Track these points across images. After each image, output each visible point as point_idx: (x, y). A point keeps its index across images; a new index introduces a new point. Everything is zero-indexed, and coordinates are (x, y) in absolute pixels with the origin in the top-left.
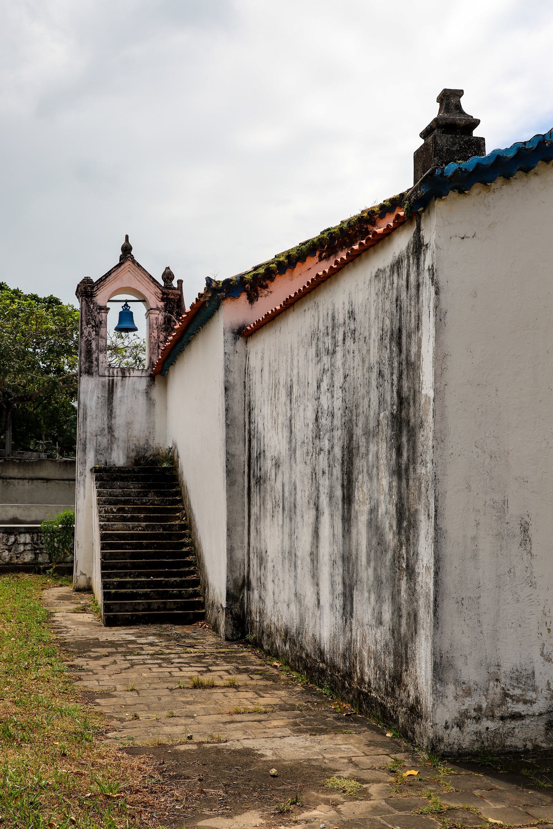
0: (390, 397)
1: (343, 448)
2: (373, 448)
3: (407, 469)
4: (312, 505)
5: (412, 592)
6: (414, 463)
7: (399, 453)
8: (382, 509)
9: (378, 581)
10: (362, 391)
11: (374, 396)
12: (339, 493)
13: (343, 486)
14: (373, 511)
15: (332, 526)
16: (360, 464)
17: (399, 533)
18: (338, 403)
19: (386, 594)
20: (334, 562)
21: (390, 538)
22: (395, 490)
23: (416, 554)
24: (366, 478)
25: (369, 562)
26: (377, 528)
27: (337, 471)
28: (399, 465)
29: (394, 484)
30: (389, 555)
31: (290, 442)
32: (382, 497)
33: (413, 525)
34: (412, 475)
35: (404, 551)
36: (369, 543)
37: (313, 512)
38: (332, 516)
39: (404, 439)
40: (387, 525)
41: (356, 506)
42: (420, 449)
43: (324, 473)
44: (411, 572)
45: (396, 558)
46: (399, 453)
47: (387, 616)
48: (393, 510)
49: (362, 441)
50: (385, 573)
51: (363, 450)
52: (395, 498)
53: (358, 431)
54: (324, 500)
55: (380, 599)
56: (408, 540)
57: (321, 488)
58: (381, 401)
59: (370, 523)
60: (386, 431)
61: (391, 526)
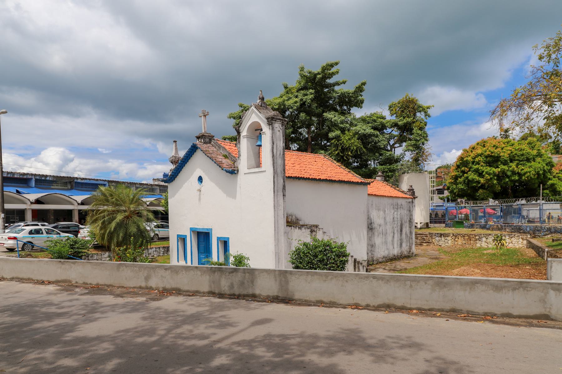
0: (409, 218)
2: (406, 224)
5: (412, 241)
7: (410, 225)
9: (407, 241)
10: (404, 216)
11: (406, 217)
12: (399, 230)
14: (406, 232)
15: (398, 235)
18: (399, 217)
19: (408, 242)
20: (398, 241)
21: (409, 235)
27: (399, 227)
31: (385, 221)
33: (412, 233)
36: (405, 237)
37: (393, 234)
38: (398, 234)
41: (403, 232)
44: (412, 238)
45: (410, 237)
46: (410, 225)
47: (408, 244)
48: (409, 232)
49: (404, 223)
50: (408, 240)
53: (403, 222)
54: (396, 232)
55: (407, 243)
58: (407, 218)
59: (405, 234)
60: (408, 222)
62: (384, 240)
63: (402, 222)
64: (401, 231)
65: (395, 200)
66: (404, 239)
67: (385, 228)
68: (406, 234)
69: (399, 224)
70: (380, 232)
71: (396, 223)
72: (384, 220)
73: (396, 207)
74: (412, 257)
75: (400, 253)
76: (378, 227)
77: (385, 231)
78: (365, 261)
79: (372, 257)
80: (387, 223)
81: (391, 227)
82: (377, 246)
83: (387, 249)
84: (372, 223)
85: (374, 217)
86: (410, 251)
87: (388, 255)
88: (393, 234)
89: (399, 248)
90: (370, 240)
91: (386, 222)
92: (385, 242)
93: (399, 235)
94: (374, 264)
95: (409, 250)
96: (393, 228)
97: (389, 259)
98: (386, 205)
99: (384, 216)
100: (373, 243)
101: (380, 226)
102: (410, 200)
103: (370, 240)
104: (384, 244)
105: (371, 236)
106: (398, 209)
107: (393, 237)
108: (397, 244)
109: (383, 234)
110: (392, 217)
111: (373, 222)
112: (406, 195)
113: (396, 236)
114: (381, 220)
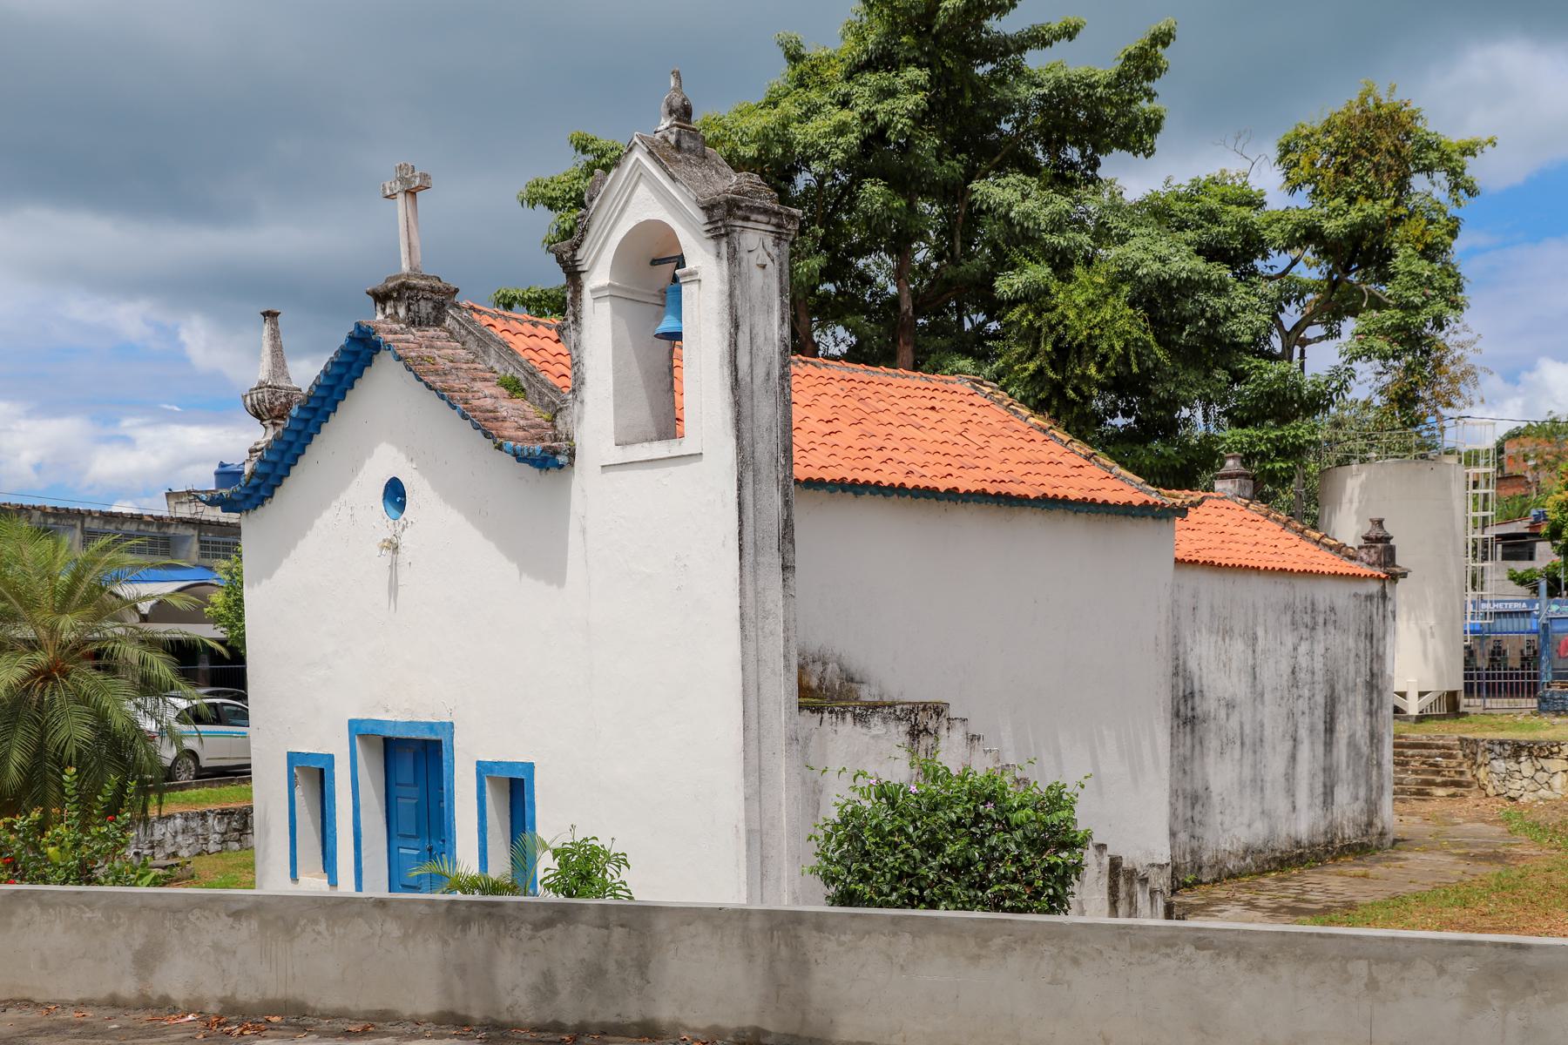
0: (1365, 670)
1: (1326, 697)
2: (1351, 699)
3: (1376, 712)
4: (1288, 737)
5: (1380, 775)
6: (1381, 708)
7: (1371, 702)
8: (1358, 735)
9: (1356, 776)
10: (1342, 662)
11: (1352, 668)
12: (1321, 727)
13: (1325, 722)
15: (1313, 750)
16: (1340, 708)
17: (1371, 746)
18: (1319, 665)
19: (1362, 782)
20: (1313, 776)
21: (1365, 750)
22: (1368, 723)
23: (1382, 755)
24: (1346, 716)
25: (1348, 767)
26: (1355, 746)
27: (1320, 712)
28: (1371, 710)
29: (1368, 719)
30: (1364, 759)
31: (1254, 686)
32: (1359, 728)
33: (1381, 741)
34: (1379, 715)
35: (1375, 756)
36: (1348, 756)
38: (1312, 743)
39: (1375, 696)
40: (1363, 744)
41: (1337, 735)
42: (1385, 701)
43: (1303, 713)
44: (1379, 765)
45: (1369, 760)
46: (1371, 702)
47: (1362, 793)
48: (1367, 734)
49: (1343, 694)
50: (1361, 770)
51: (1343, 699)
52: (1368, 727)
53: (1339, 687)
55: (1357, 786)
56: (1377, 749)
57: (1300, 725)
58: (1357, 672)
59: (1349, 744)
60: (1361, 689)
61: (1365, 743)
62: (1247, 773)
63: (1333, 689)
64: (1330, 729)
65: (1303, 589)
66: (1344, 766)
67: (1254, 716)
68: (1352, 744)
69: (1320, 699)
70: (1231, 735)
71: (1306, 693)
72: (1250, 680)
73: (1307, 619)
74: (1378, 849)
75: (1326, 833)
76: (1223, 713)
77: (1255, 731)
78: (1161, 867)
79: (1193, 852)
80: (1262, 695)
81: (1284, 711)
82: (1216, 799)
83: (1263, 812)
84: (1192, 694)
85: (1204, 664)
86: (1370, 824)
87: (1266, 843)
88: (1291, 743)
89: (1320, 812)
90: (1185, 772)
91: (1259, 688)
92: (1254, 780)
93: (1320, 749)
94: (1201, 882)
95: (1364, 819)
96: (1291, 714)
97: (1274, 859)
98: (1261, 612)
99: (1250, 662)
100: (1199, 785)
101: (1230, 705)
102: (1374, 587)
103: (1185, 772)
104: (1248, 791)
105: (1188, 753)
106: (1313, 629)
107: (1293, 758)
108: (1312, 790)
109: (1242, 744)
110: (1285, 668)
111: (1196, 687)
112: (1353, 564)
113: (1304, 753)
114: (1235, 679)
